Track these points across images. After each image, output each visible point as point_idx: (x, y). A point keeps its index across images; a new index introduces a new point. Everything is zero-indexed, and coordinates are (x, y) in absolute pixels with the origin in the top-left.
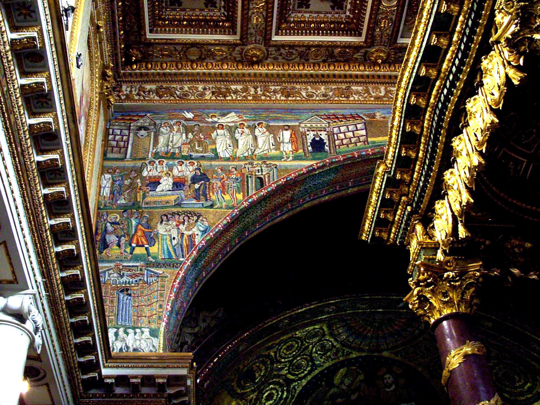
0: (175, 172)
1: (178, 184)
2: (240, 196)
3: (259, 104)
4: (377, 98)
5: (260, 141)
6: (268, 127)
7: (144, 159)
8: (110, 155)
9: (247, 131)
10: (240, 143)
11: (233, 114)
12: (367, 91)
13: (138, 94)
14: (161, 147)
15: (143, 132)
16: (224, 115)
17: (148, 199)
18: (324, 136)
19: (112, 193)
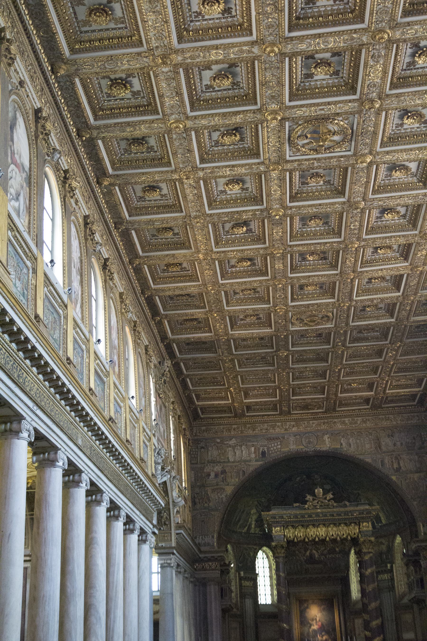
0: (215, 469)
1: (216, 475)
2: (237, 480)
3: (243, 435)
4: (286, 430)
5: (244, 452)
6: (246, 445)
7: (204, 463)
8: (192, 462)
9: (239, 447)
10: (237, 454)
11: (234, 439)
12: (282, 425)
13: (199, 433)
14: (210, 458)
15: (203, 450)
16: (231, 440)
17: (207, 483)
18: (266, 450)
19: (195, 480)
